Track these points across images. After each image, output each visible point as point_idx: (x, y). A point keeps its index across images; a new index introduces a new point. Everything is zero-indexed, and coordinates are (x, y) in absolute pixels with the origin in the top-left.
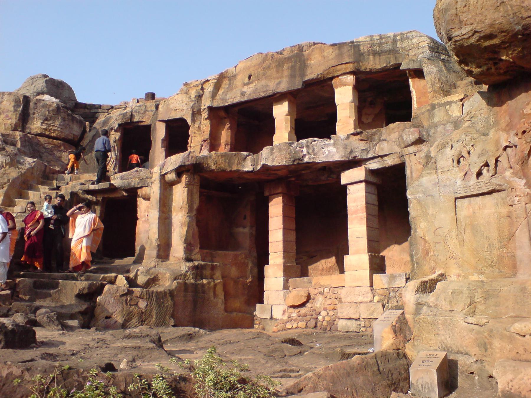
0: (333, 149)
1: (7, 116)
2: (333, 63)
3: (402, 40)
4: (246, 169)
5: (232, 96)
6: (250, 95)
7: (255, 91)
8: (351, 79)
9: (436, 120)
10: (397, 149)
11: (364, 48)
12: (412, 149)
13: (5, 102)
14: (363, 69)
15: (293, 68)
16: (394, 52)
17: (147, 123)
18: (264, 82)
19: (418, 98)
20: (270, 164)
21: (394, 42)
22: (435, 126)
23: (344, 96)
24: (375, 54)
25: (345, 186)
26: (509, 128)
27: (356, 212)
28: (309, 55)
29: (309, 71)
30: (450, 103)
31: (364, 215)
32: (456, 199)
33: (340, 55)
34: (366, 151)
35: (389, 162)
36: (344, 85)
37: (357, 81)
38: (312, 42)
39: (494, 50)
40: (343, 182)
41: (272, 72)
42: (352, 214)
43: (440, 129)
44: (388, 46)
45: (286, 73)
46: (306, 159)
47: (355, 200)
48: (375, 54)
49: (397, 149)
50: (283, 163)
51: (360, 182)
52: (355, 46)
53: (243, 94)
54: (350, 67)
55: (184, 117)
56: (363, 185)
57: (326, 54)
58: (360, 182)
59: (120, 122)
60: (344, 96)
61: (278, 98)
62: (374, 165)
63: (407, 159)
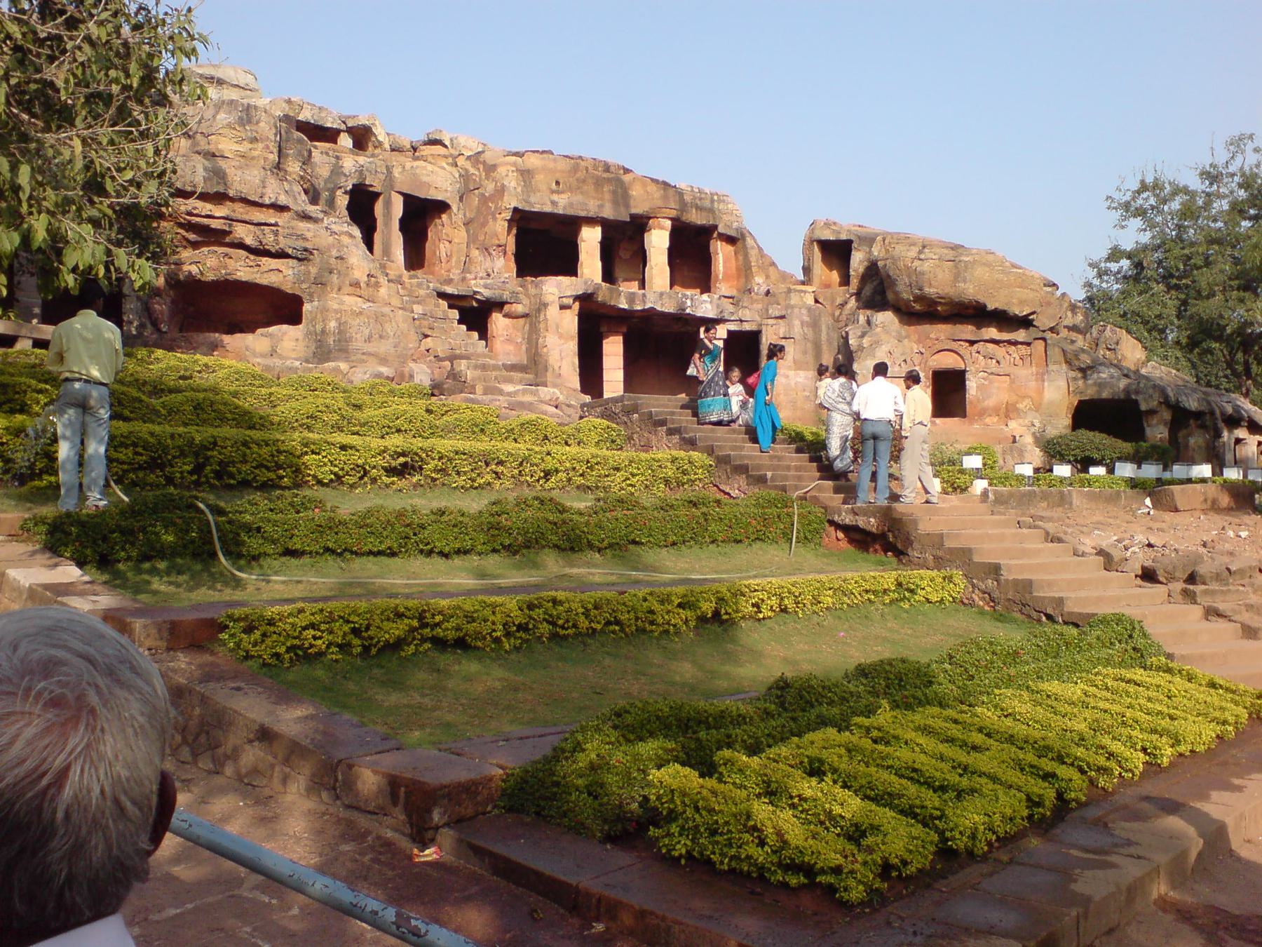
0: (709, 306)
1: (268, 147)
2: (659, 203)
3: (719, 201)
4: (622, 306)
5: (542, 202)
6: (565, 208)
7: (571, 205)
8: (668, 223)
9: (792, 302)
10: (758, 319)
11: (687, 198)
12: (771, 321)
13: (262, 124)
14: (684, 219)
15: (614, 193)
16: (711, 211)
17: (378, 189)
18: (577, 198)
19: (724, 262)
20: (659, 308)
21: (712, 201)
22: (792, 307)
23: (658, 241)
24: (699, 208)
26: (919, 342)
28: (630, 183)
29: (632, 203)
30: (805, 292)
33: (665, 197)
34: (732, 313)
35: (747, 327)
36: (662, 228)
37: (673, 226)
38: (621, 164)
39: (936, 303)
41: (590, 188)
43: (796, 310)
44: (707, 204)
45: (607, 196)
46: (688, 311)
48: (699, 208)
49: (758, 319)
50: (671, 311)
52: (680, 194)
53: (554, 203)
54: (673, 214)
57: (649, 189)
59: (355, 181)
60: (658, 241)
61: (591, 221)
62: (733, 327)
63: (764, 328)
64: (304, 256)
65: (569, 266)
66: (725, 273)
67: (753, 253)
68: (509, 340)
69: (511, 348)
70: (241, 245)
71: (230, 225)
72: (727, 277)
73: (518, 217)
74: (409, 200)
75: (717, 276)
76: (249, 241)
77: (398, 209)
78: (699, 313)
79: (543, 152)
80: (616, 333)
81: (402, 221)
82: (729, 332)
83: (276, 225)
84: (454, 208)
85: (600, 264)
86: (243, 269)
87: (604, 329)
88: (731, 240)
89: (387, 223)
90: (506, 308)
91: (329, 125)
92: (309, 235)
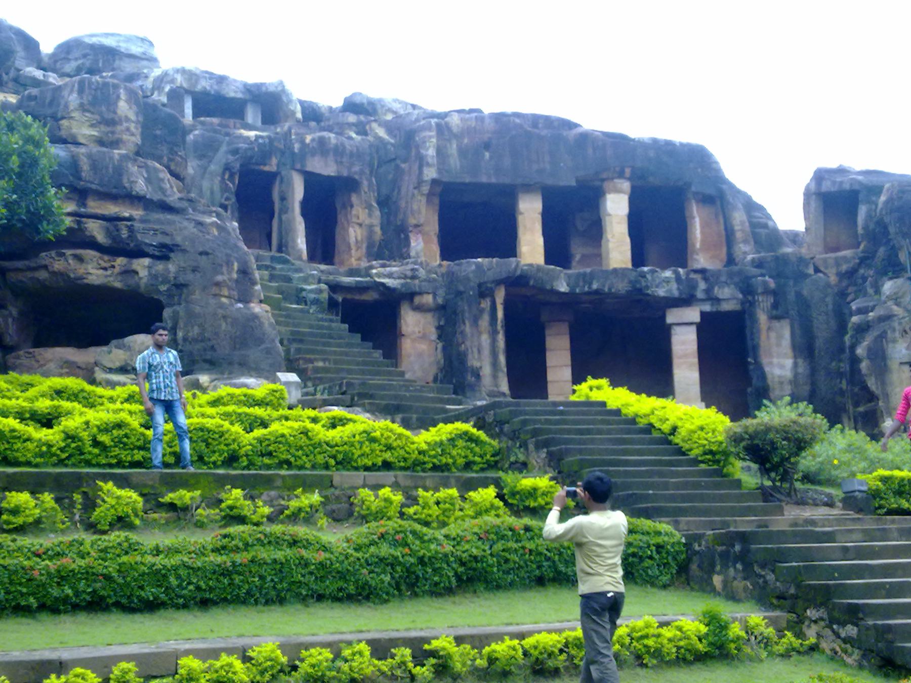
1: (128, 129)
8: (626, 185)
19: (702, 227)
23: (616, 207)
25: (671, 325)
27: (686, 356)
31: (696, 360)
32: (901, 363)
37: (633, 188)
40: (670, 319)
42: (680, 358)
47: (683, 343)
51: (691, 324)
55: (357, 177)
56: (693, 329)
58: (691, 324)
60: (616, 207)
62: (707, 308)
64: (164, 252)
65: (507, 245)
66: (702, 241)
67: (739, 218)
68: (424, 337)
69: (423, 347)
70: (92, 244)
71: (79, 223)
72: (707, 246)
73: (438, 189)
74: (311, 180)
75: (694, 245)
76: (101, 238)
77: (298, 191)
78: (661, 292)
79: (472, 111)
80: (563, 321)
81: (304, 204)
82: (703, 314)
83: (130, 219)
84: (365, 184)
85: (540, 241)
86: (94, 271)
87: (544, 318)
88: (707, 200)
89: (285, 210)
90: (417, 300)
91: (232, 95)
92: (167, 228)
